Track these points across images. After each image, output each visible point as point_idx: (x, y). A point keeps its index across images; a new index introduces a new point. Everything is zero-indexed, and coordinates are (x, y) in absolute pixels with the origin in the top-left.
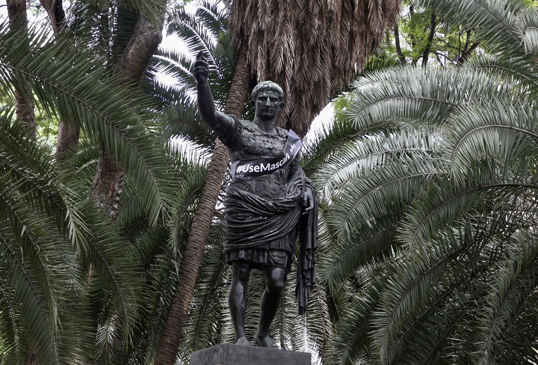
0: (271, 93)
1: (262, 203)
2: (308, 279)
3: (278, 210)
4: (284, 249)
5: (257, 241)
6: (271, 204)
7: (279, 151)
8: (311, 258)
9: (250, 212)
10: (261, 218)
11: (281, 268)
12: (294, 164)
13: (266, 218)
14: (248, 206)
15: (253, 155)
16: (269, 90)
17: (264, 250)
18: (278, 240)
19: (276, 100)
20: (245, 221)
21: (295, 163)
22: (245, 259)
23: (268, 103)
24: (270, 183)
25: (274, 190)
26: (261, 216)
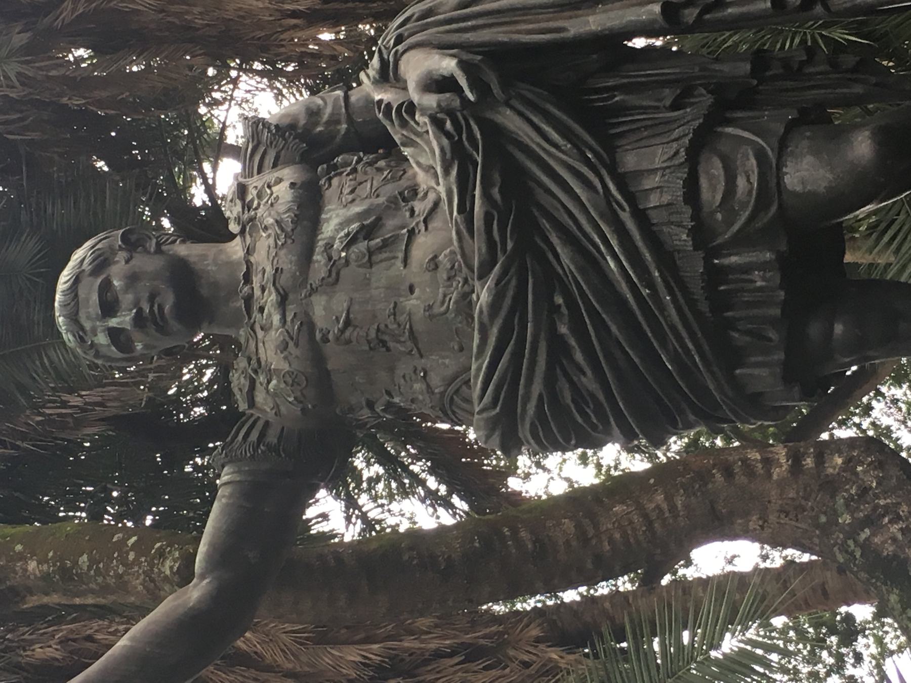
0: (88, 318)
1: (494, 331)
4: (683, 174)
5: (673, 328)
6: (483, 296)
7: (282, 253)
9: (550, 381)
10: (563, 329)
11: (779, 168)
12: (344, 126)
13: (559, 300)
16: (82, 328)
19: (106, 286)
20: (601, 397)
21: (338, 122)
22: (780, 356)
23: (123, 320)
24: (411, 289)
25: (437, 267)
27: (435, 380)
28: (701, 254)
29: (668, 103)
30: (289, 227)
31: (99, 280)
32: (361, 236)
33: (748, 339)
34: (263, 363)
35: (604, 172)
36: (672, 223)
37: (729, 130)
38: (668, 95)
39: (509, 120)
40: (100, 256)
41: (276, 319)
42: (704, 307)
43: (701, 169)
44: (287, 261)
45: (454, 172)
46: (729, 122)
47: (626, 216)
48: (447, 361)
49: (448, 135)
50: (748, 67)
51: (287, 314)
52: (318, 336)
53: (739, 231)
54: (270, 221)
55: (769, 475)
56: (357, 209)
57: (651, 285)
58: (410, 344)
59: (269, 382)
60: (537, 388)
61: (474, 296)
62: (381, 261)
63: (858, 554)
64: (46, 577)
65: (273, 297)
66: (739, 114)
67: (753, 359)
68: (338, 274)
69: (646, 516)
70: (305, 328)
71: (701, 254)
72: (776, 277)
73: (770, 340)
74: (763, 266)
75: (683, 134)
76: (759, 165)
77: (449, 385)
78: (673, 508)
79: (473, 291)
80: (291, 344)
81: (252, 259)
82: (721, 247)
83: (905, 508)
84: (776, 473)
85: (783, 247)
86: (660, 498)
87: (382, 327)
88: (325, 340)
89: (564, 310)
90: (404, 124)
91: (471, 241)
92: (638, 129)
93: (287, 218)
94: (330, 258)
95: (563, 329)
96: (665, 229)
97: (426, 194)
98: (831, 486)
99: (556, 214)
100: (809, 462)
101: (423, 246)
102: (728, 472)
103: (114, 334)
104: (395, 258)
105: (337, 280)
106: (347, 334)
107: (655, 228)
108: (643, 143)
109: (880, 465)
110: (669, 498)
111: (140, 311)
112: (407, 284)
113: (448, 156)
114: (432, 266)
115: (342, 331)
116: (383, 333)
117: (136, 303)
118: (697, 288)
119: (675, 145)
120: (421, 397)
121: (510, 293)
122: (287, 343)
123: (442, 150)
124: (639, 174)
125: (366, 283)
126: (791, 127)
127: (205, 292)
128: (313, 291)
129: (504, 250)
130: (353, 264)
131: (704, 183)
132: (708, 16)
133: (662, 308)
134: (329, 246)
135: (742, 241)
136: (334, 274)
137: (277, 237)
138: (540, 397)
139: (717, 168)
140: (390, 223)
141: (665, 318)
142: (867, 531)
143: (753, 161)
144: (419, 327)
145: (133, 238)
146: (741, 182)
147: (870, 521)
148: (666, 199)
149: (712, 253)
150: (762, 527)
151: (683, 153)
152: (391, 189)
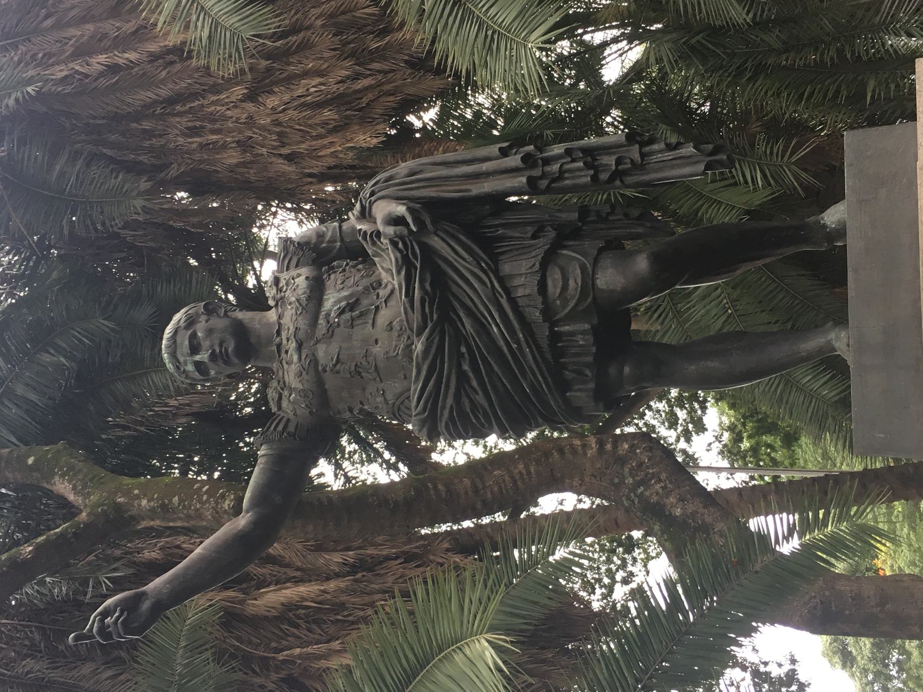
0: (183, 355)
2: (619, 162)
3: (435, 317)
4: (537, 277)
6: (419, 347)
7: (300, 318)
8: (555, 167)
10: (466, 367)
12: (339, 244)
13: (463, 350)
14: (443, 407)
15: (325, 391)
17: (555, 337)
18: (521, 302)
19: (194, 336)
21: (336, 242)
22: (592, 385)
24: (376, 342)
26: (459, 365)
27: (389, 396)
28: (547, 324)
29: (529, 235)
30: (304, 303)
31: (189, 332)
32: (347, 309)
33: (574, 375)
34: (287, 384)
35: (492, 275)
36: (531, 306)
37: (565, 252)
38: (530, 230)
39: (436, 242)
40: (191, 317)
41: (295, 358)
42: (549, 356)
43: (548, 274)
44: (303, 323)
45: (403, 273)
46: (565, 247)
47: (504, 301)
48: (397, 385)
49: (400, 251)
50: (577, 215)
51: (302, 354)
52: (320, 368)
53: (570, 311)
54: (294, 299)
55: (586, 454)
56: (345, 293)
57: (518, 342)
58: (375, 374)
59: (290, 395)
60: (450, 401)
61: (414, 347)
62: (359, 325)
63: (636, 502)
64: (152, 510)
65: (294, 344)
66: (571, 243)
67: (577, 387)
68: (333, 331)
69: (512, 477)
70: (312, 364)
71: (547, 324)
72: (590, 338)
73: (587, 376)
74: (583, 333)
75: (540, 253)
76: (582, 273)
77: (397, 399)
78: (529, 473)
79: (413, 344)
80: (304, 373)
81: (282, 322)
82: (558, 320)
83: (664, 475)
84: (589, 453)
85: (595, 321)
86: (521, 466)
87: (358, 363)
88: (325, 371)
89: (466, 356)
90: (374, 244)
91: (412, 314)
92: (511, 250)
93: (303, 298)
94: (328, 322)
95: (466, 367)
96: (527, 309)
97: (386, 285)
98: (622, 461)
99: (463, 299)
100: (609, 447)
101: (384, 316)
102: (561, 451)
103: (198, 365)
104: (367, 323)
105: (333, 334)
106: (338, 367)
107: (521, 309)
108: (514, 258)
109: (650, 449)
110: (527, 467)
111: (214, 352)
112: (374, 339)
113: (400, 263)
114: (389, 328)
115: (335, 366)
116: (360, 367)
117: (212, 347)
118: (544, 343)
119: (533, 260)
120: (381, 406)
121: (435, 346)
122: (302, 373)
123: (396, 259)
124: (511, 276)
125: (350, 337)
126: (601, 251)
127: (253, 340)
128: (318, 342)
129: (432, 321)
130: (342, 326)
131: (550, 283)
132: (553, 185)
133: (524, 356)
134: (328, 315)
135: (571, 317)
136: (330, 332)
137: (297, 309)
138: (452, 407)
139: (558, 275)
140: (365, 302)
141: (526, 363)
142: (642, 488)
143: (579, 271)
144: (378, 363)
145: (211, 307)
146: (571, 283)
147: (644, 482)
148: (527, 291)
149: (553, 324)
150: (581, 485)
151: (538, 265)
152: (365, 282)
